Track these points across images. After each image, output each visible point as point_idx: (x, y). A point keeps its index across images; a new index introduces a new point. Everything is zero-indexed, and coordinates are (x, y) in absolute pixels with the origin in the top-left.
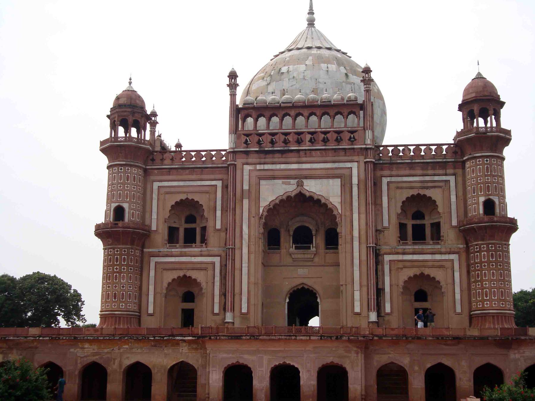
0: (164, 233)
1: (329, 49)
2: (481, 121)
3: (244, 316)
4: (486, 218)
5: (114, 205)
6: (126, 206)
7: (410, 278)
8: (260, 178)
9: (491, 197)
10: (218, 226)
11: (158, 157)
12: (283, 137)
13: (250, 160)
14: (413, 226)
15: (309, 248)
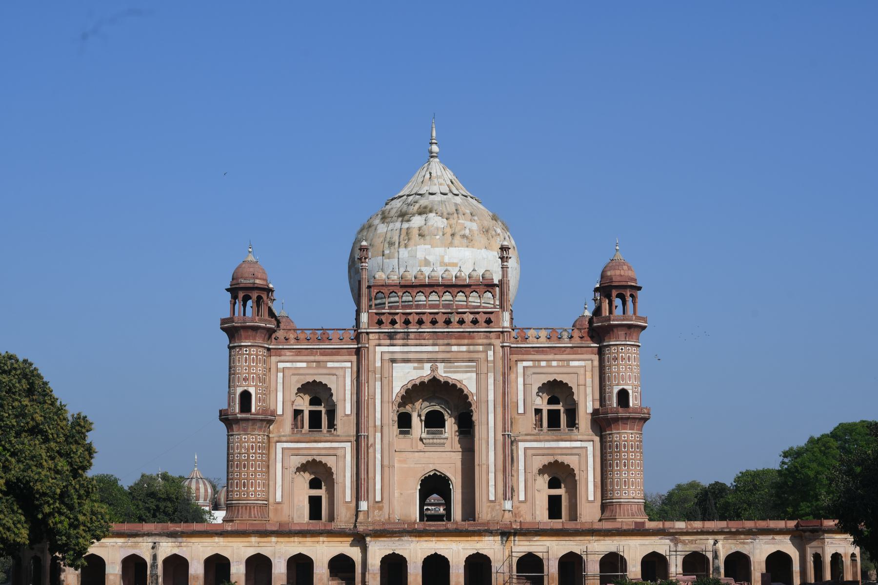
0: (289, 415)
1: (457, 195)
2: (618, 302)
3: (378, 505)
4: (620, 410)
5: (239, 390)
6: (252, 390)
7: (544, 466)
8: (393, 361)
9: (625, 387)
10: (348, 412)
11: (280, 334)
12: (417, 318)
13: (382, 342)
14: (549, 410)
15: (441, 433)
